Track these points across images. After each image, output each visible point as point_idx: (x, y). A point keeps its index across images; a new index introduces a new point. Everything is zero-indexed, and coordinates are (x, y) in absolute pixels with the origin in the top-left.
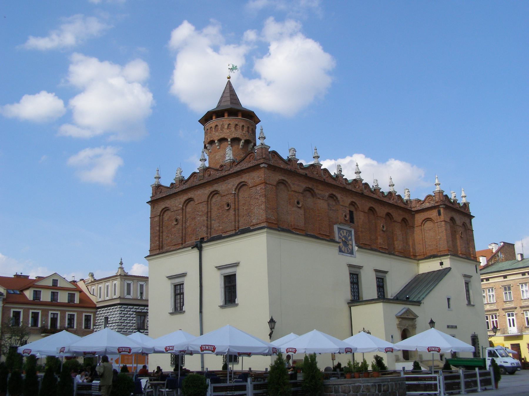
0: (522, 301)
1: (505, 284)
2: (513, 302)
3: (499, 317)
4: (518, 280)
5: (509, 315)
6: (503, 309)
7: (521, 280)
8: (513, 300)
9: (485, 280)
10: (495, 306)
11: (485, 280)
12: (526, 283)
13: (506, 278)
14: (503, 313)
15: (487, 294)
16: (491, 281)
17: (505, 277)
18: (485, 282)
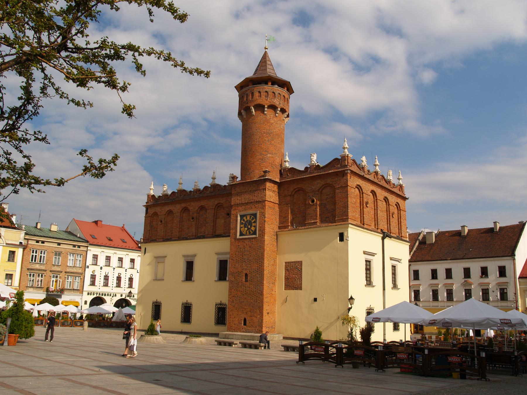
0: (68, 267)
1: (57, 250)
2: (60, 267)
3: (45, 277)
4: (69, 250)
5: (53, 277)
6: (51, 271)
7: (71, 250)
8: (60, 265)
9: (40, 242)
10: (45, 267)
11: (40, 242)
12: (75, 254)
13: (60, 245)
14: (49, 273)
15: (39, 254)
16: (46, 244)
17: (74, 246)
18: (40, 244)
